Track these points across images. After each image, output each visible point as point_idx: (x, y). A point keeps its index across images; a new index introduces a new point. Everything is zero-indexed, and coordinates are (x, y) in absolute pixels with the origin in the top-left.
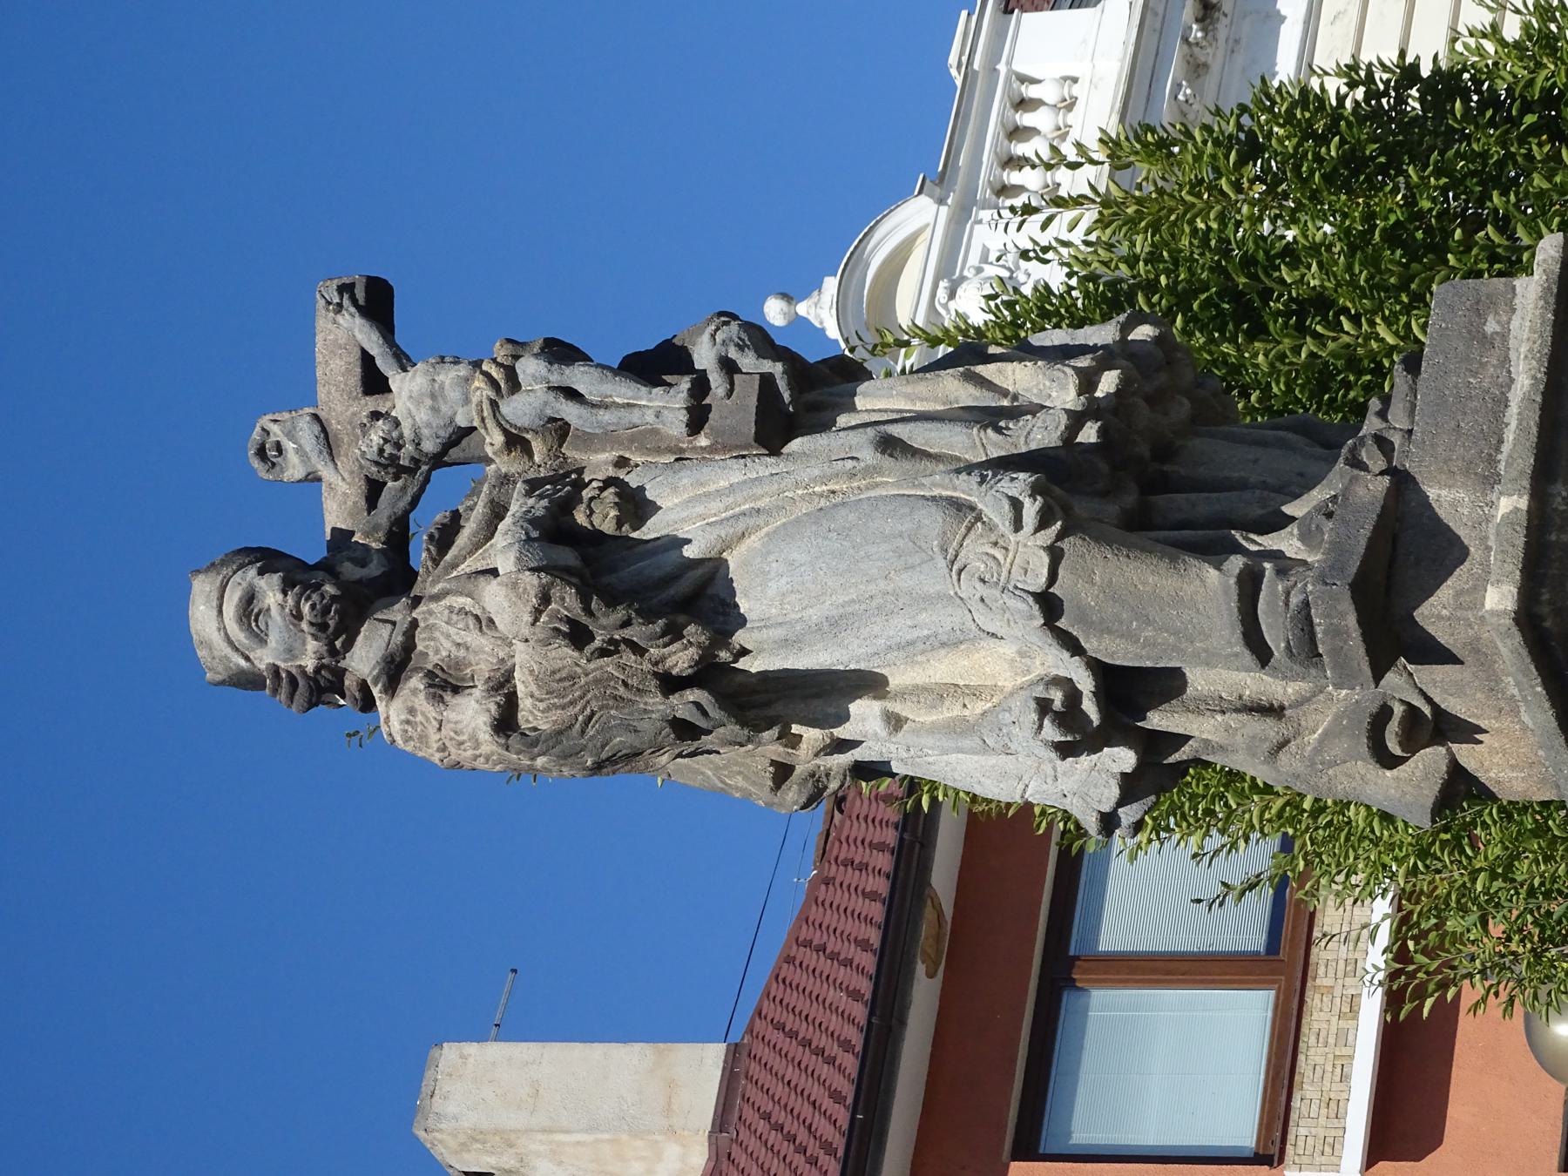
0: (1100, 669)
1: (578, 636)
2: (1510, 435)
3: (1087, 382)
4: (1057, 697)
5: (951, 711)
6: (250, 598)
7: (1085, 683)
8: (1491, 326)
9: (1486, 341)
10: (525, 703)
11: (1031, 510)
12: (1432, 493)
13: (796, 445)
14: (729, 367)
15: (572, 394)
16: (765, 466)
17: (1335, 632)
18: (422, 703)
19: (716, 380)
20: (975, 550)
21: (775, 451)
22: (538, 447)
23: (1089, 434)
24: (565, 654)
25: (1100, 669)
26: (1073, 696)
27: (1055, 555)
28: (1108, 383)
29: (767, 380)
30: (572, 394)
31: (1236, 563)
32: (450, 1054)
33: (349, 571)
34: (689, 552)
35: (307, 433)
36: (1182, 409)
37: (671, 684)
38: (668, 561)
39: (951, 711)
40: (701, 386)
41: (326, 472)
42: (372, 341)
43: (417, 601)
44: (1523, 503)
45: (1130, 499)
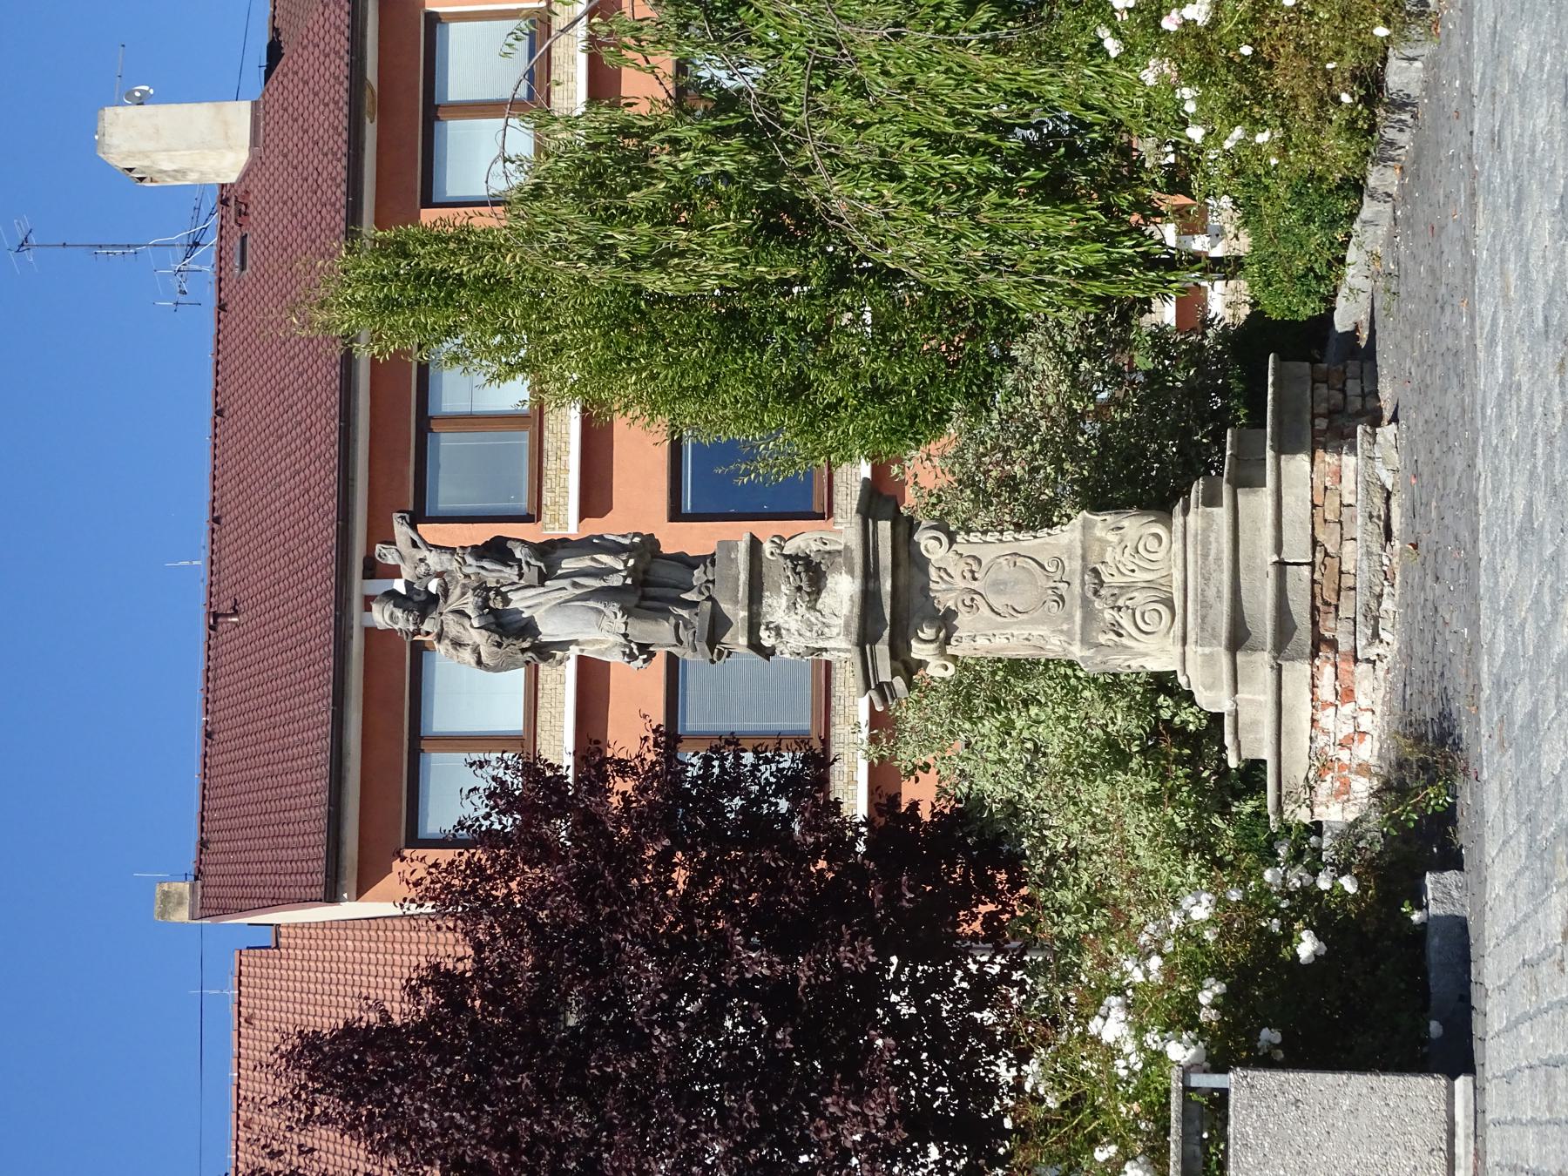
0: (637, 644)
1: (499, 645)
2: (741, 589)
3: (626, 562)
4: (627, 651)
5: (597, 647)
6: (392, 615)
7: (634, 647)
8: (733, 556)
9: (732, 560)
10: (484, 659)
11: (619, 615)
12: (722, 606)
13: (548, 583)
14: (528, 564)
15: (483, 568)
16: (542, 590)
17: (703, 650)
18: (450, 648)
19: (524, 565)
20: (605, 624)
21: (543, 586)
22: (473, 577)
23: (629, 581)
24: (496, 649)
25: (637, 644)
26: (631, 649)
27: (626, 624)
28: (631, 562)
29: (540, 568)
30: (483, 568)
31: (673, 621)
32: (109, 112)
33: (416, 598)
34: (524, 616)
35: (396, 555)
36: (649, 556)
37: (523, 651)
38: (517, 617)
39: (597, 647)
40: (521, 568)
41: (402, 565)
42: (416, 538)
43: (441, 614)
44: (746, 614)
45: (639, 593)
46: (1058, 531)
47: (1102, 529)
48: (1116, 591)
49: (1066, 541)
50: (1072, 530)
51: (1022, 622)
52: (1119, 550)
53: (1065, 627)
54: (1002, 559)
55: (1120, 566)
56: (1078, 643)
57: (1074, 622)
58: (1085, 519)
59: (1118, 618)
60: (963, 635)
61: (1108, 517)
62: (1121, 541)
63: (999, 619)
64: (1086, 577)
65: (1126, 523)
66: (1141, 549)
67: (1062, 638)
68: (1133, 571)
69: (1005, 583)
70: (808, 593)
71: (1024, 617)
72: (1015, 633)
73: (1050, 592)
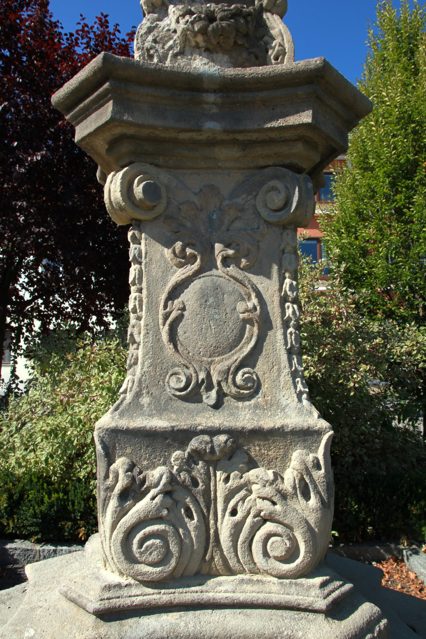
46: (300, 386)
47: (303, 462)
48: (201, 486)
49: (284, 402)
50: (300, 411)
51: (158, 333)
52: (269, 491)
53: (145, 400)
54: (254, 301)
55: (243, 493)
56: (113, 425)
57: (151, 416)
58: (319, 433)
59: (153, 492)
60: (143, 247)
61: (323, 471)
62: (284, 496)
63: (163, 297)
64: (223, 438)
65: (313, 501)
66: (269, 527)
67: (129, 396)
68: (234, 513)
69: (218, 305)
70: (203, 31)
71: (165, 336)
72: (142, 322)
73: (202, 376)
